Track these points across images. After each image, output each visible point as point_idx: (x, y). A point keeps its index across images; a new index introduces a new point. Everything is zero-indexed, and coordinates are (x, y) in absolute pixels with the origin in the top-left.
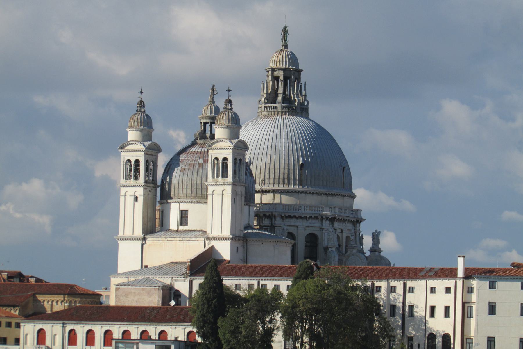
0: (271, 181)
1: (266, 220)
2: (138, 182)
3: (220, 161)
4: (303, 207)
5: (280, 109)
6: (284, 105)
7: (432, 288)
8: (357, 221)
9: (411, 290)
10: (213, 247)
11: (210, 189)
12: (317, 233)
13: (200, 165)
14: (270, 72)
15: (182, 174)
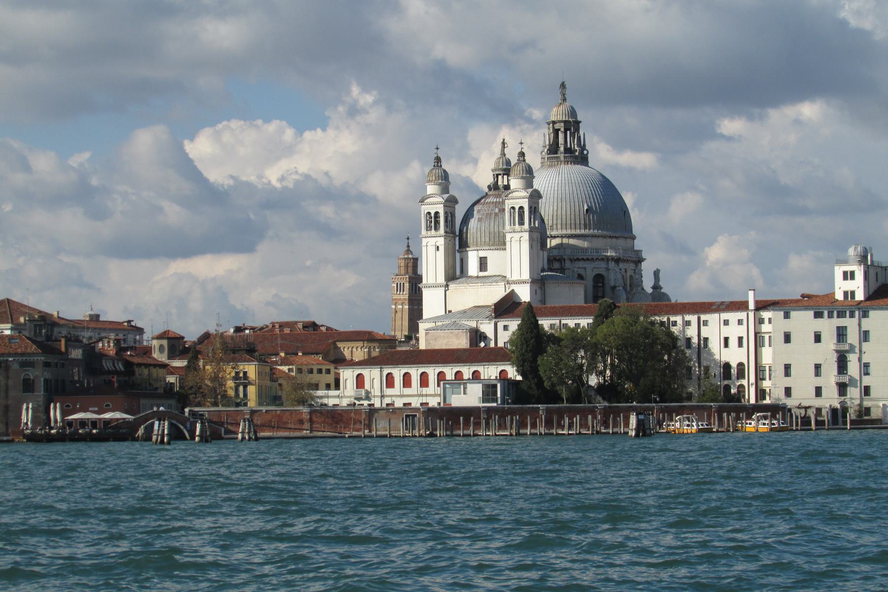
0: (559, 226)
1: (556, 263)
2: (438, 233)
3: (517, 210)
4: (590, 250)
5: (562, 158)
6: (566, 155)
7: (725, 321)
8: (639, 261)
9: (706, 323)
10: (513, 290)
11: (508, 236)
12: (604, 273)
13: (496, 214)
14: (551, 125)
15: (479, 223)
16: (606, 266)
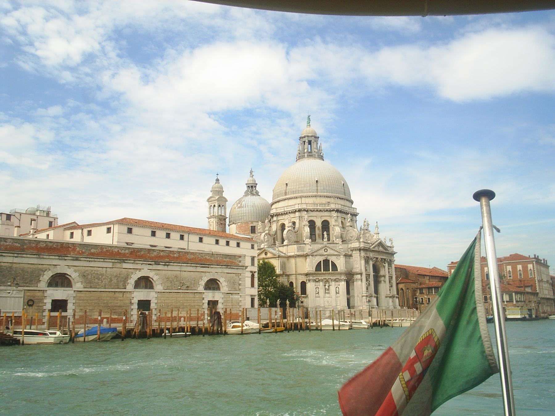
4: (319, 205)
16: (330, 215)
